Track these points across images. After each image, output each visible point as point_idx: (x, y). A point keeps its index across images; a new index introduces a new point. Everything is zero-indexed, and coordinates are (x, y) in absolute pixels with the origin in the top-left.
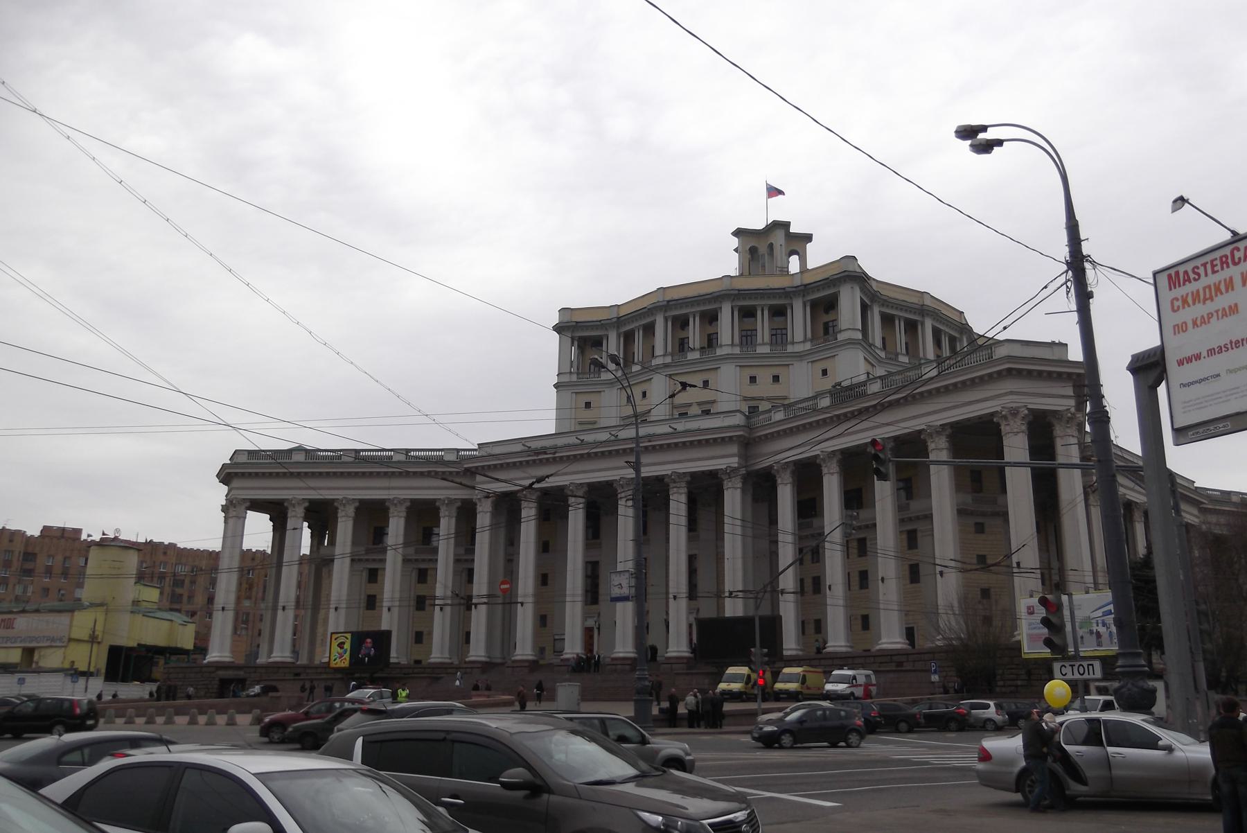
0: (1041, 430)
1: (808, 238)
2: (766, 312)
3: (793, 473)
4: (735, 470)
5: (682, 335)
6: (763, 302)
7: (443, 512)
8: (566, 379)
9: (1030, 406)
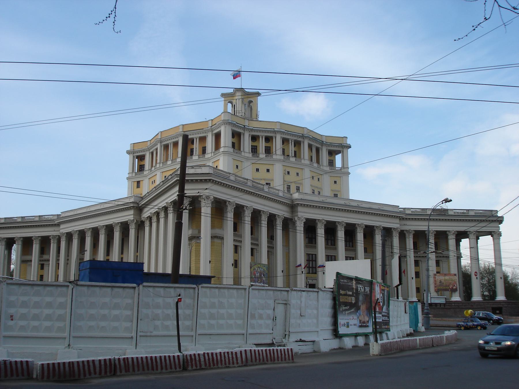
2: (198, 140)
8: (131, 175)
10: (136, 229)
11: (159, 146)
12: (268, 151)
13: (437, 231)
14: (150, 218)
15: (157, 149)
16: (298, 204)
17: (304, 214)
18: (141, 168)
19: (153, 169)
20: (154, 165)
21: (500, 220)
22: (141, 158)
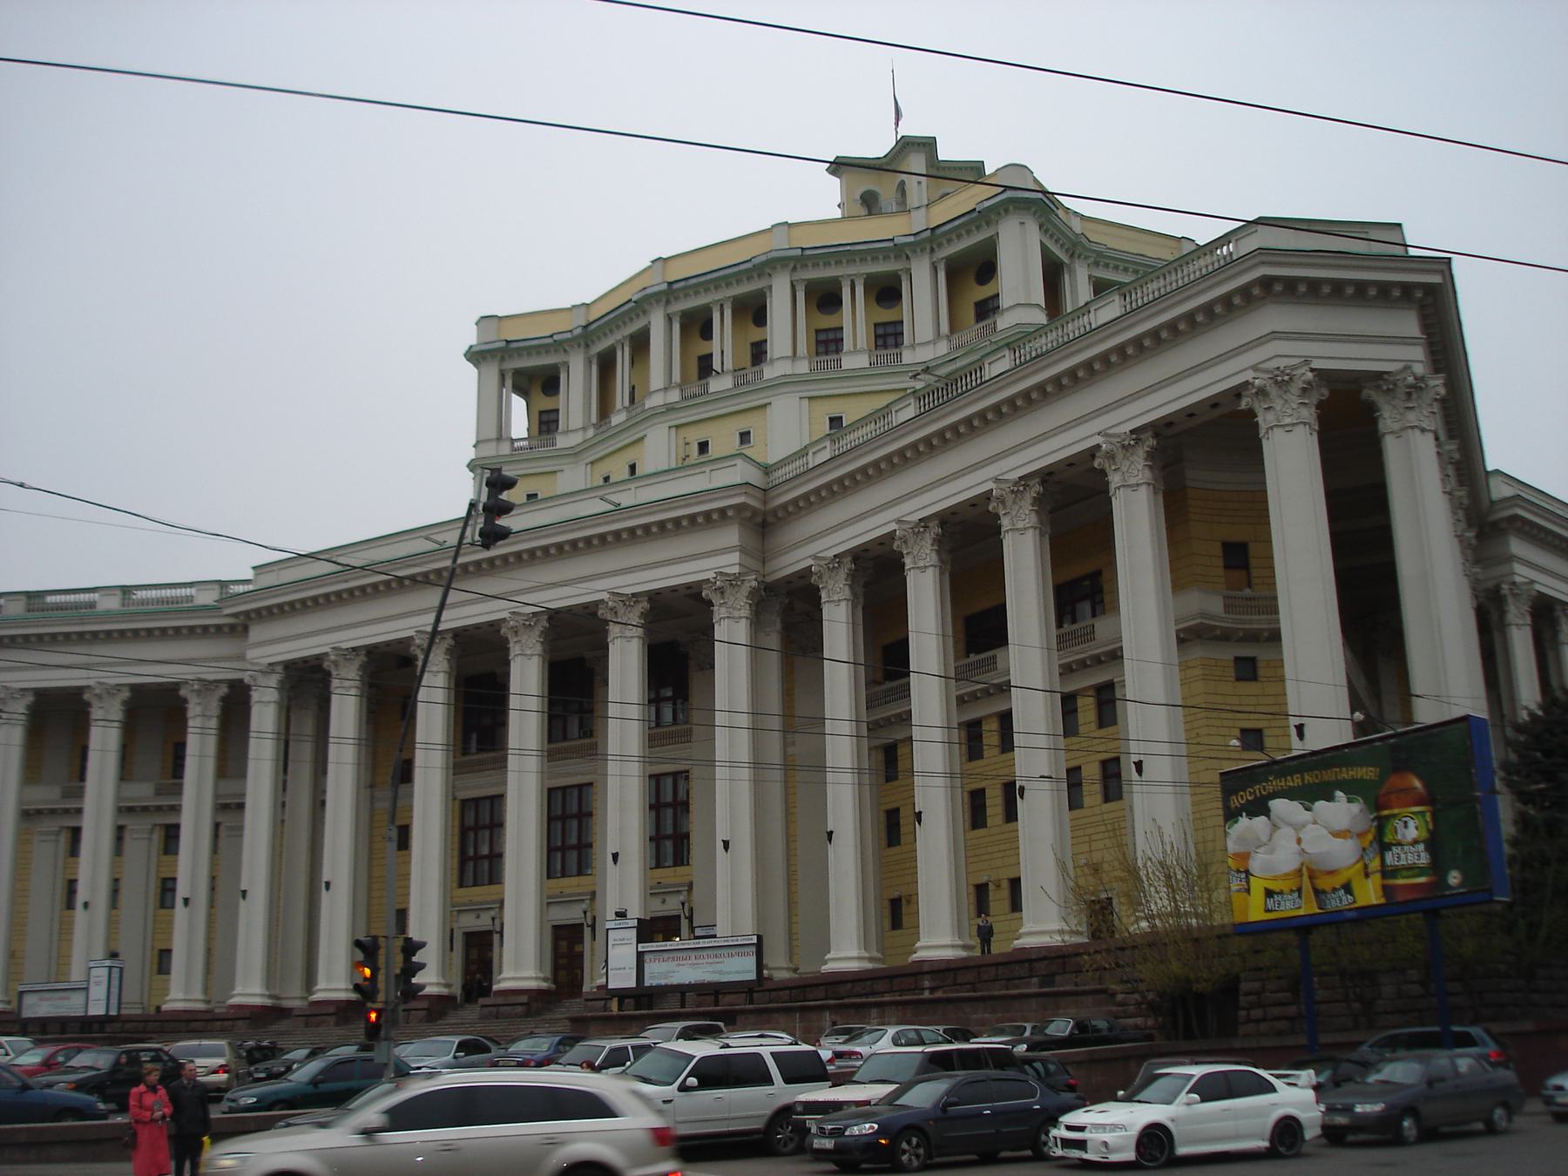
0: (1348, 423)
2: (860, 290)
3: (853, 577)
4: (734, 581)
5: (702, 348)
6: (852, 270)
7: (194, 709)
8: (490, 450)
9: (1316, 364)
11: (657, 322)
16: (1516, 517)
19: (617, 419)
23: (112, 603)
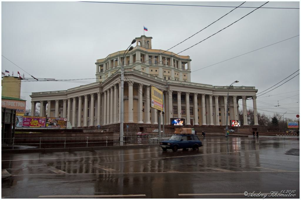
1: (151, 38)
8: (97, 73)
10: (100, 96)
11: (109, 61)
12: (157, 62)
13: (238, 96)
14: (106, 91)
15: (108, 62)
17: (172, 89)
18: (102, 70)
19: (107, 70)
20: (107, 69)
21: (256, 91)
22: (102, 66)
23: (57, 92)
